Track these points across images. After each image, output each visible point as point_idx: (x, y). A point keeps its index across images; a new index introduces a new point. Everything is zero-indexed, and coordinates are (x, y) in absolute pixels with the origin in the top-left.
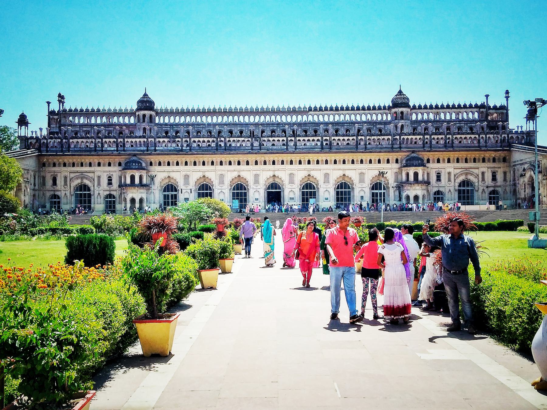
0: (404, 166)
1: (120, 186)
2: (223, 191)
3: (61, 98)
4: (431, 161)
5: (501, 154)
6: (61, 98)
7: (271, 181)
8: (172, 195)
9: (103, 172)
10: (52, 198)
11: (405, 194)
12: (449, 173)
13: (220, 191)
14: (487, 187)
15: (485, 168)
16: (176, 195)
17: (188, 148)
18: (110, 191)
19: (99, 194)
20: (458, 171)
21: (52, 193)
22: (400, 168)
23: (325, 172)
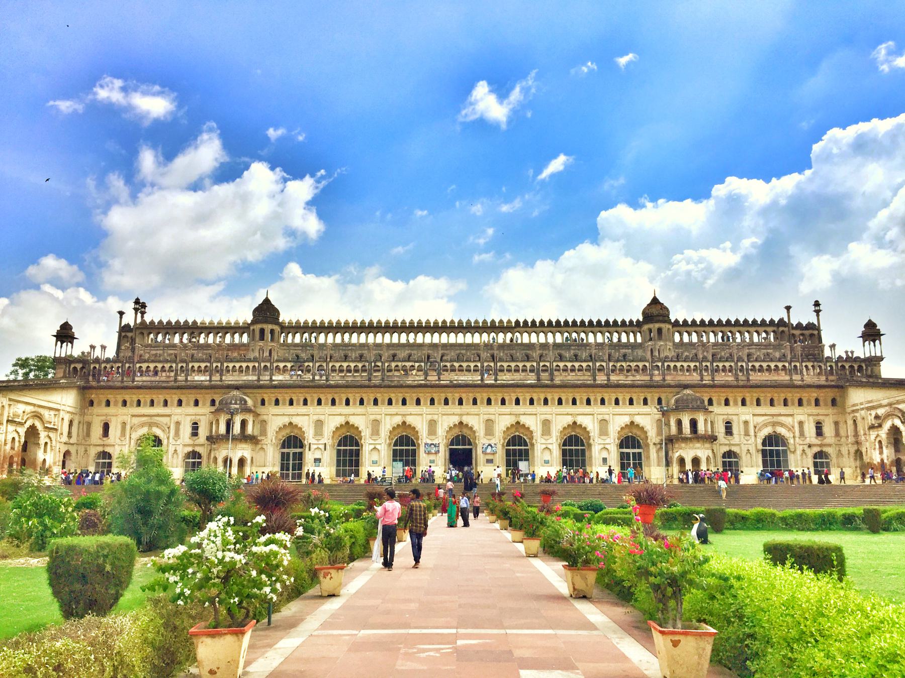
0: (673, 410)
1: (210, 438)
2: (378, 447)
4: (715, 402)
5: (829, 394)
7: (456, 431)
8: (294, 454)
9: (185, 415)
10: (99, 458)
11: (677, 455)
12: (746, 423)
13: (372, 447)
14: (810, 446)
16: (301, 454)
19: (176, 451)
20: (761, 419)
21: (100, 449)
23: (543, 417)
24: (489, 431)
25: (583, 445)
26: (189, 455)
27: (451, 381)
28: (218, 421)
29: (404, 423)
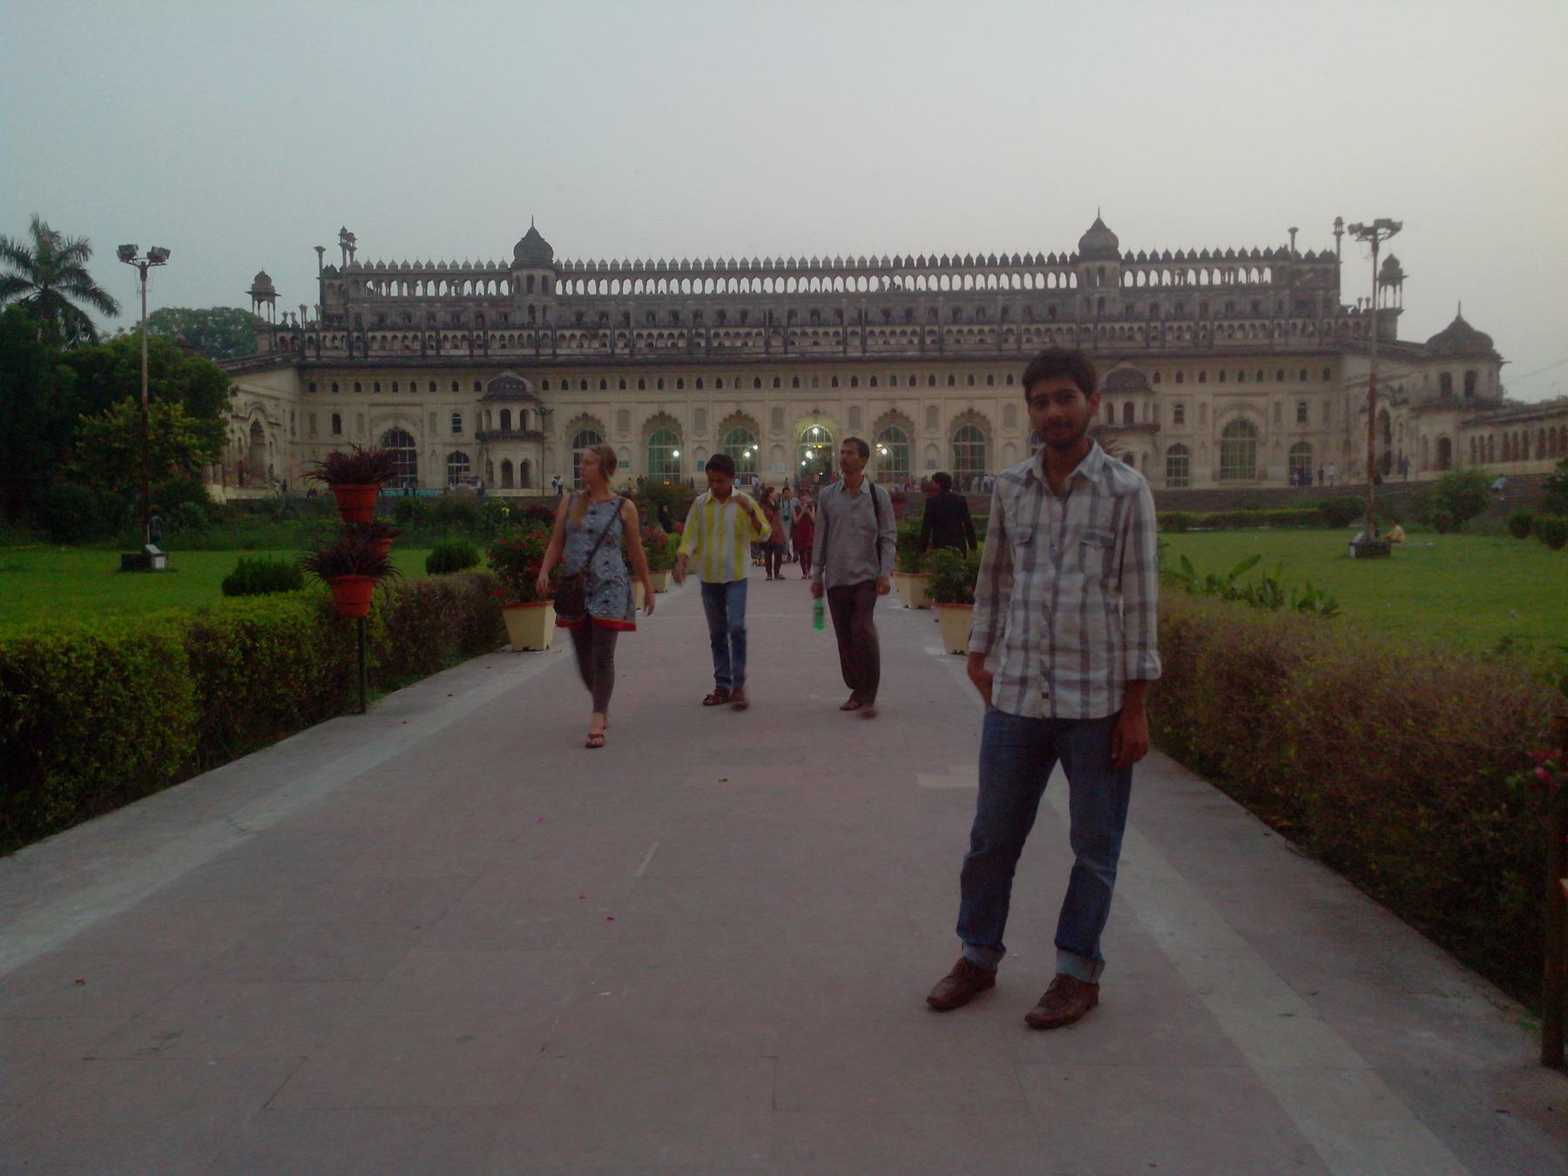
3: (347, 240)
6: (347, 240)
12: (1203, 406)
17: (627, 351)
18: (457, 444)
20: (1224, 401)
25: (981, 439)
26: (451, 458)
27: (802, 354)
28: (489, 413)
29: (739, 412)
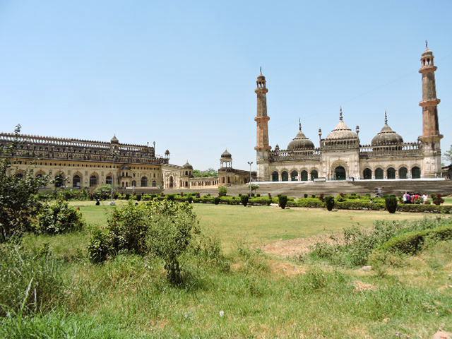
15: (152, 172)
22: (120, 171)
24: (69, 174)
